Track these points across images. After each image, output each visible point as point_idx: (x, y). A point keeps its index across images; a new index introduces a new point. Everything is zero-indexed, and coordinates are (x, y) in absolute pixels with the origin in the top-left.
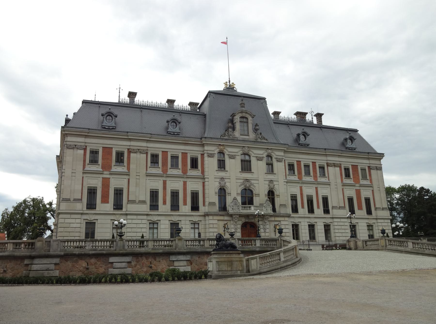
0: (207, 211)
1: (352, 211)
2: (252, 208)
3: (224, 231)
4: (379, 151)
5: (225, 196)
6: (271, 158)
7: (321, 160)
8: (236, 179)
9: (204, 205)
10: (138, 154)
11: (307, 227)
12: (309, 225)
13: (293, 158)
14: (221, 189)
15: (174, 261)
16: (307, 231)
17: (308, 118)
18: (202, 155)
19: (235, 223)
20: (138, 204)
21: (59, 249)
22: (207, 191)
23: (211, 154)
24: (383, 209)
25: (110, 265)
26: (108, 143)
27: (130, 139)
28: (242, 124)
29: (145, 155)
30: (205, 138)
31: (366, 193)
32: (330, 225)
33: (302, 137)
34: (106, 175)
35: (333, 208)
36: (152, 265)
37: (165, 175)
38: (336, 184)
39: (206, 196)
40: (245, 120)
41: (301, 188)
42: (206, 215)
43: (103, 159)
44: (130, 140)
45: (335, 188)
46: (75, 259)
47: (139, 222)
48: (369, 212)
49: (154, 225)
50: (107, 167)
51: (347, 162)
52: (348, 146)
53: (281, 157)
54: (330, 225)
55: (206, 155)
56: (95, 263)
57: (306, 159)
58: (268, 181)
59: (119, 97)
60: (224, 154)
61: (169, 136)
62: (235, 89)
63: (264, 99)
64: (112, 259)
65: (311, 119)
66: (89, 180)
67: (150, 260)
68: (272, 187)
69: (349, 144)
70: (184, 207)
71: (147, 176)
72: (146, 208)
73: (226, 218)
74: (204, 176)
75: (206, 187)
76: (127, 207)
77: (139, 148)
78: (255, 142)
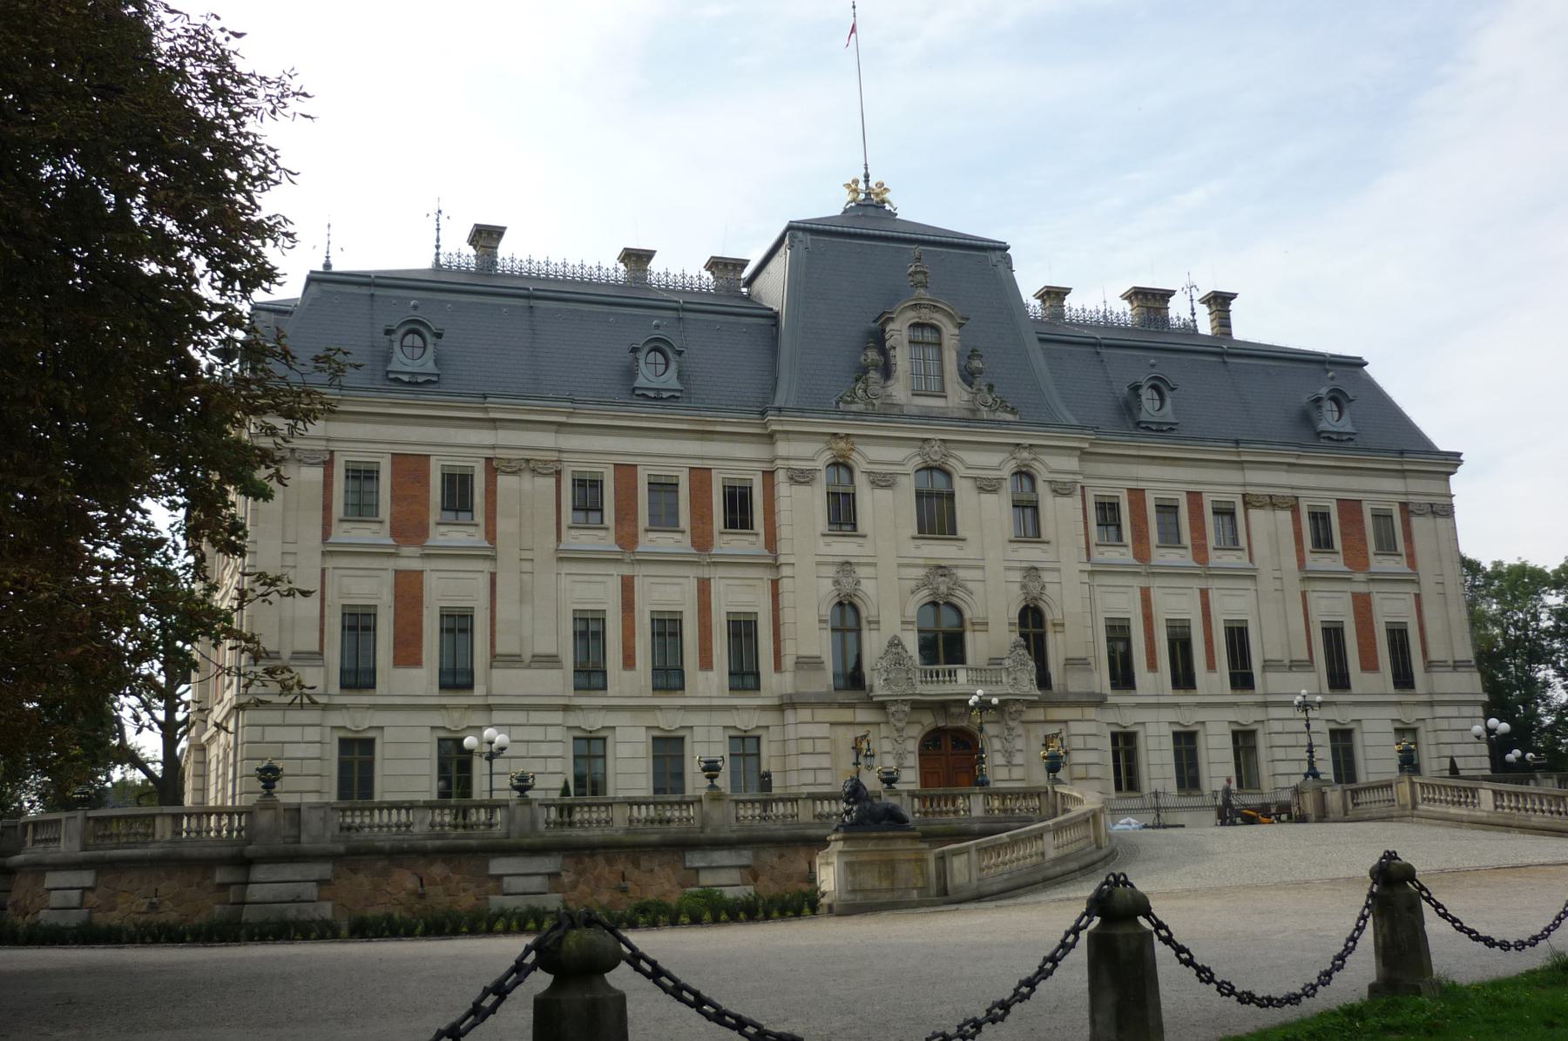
0: (790, 690)
1: (1339, 679)
2: (962, 676)
3: (857, 764)
4: (1443, 446)
5: (858, 631)
6: (1032, 478)
7: (1221, 484)
8: (900, 565)
9: (778, 667)
10: (527, 476)
11: (1169, 743)
12: (1177, 736)
13: (1113, 479)
14: (840, 604)
15: (697, 870)
16: (1169, 757)
17: (1178, 310)
18: (769, 475)
19: (896, 734)
20: (529, 667)
21: (328, 835)
22: (787, 616)
23: (802, 471)
24: (1457, 666)
25: (491, 884)
26: (412, 437)
27: (494, 420)
28: (919, 350)
29: (552, 481)
30: (780, 409)
31: (1391, 607)
32: (1253, 733)
33: (1147, 394)
34: (410, 561)
35: (1267, 665)
36: (629, 884)
37: (627, 557)
38: (1278, 574)
39: (786, 632)
40: (928, 336)
41: (1146, 595)
42: (786, 705)
43: (394, 498)
44: (494, 423)
45: (1272, 592)
46: (380, 864)
47: (537, 734)
48: (1403, 679)
50: (409, 529)
51: (1322, 487)
52: (1323, 426)
53: (1069, 478)
54: (1253, 733)
55: (781, 476)
56: (446, 879)
57: (1164, 480)
58: (1021, 569)
59: (438, 247)
60: (850, 470)
61: (643, 406)
62: (888, 207)
63: (1003, 248)
64: (498, 866)
65: (1187, 316)
66: (346, 581)
67: (620, 867)
68: (1035, 593)
69: (1329, 420)
70: (701, 675)
71: (560, 559)
72: (557, 682)
73: (863, 715)
74: (776, 559)
75: (786, 600)
76: (491, 682)
78: (968, 420)
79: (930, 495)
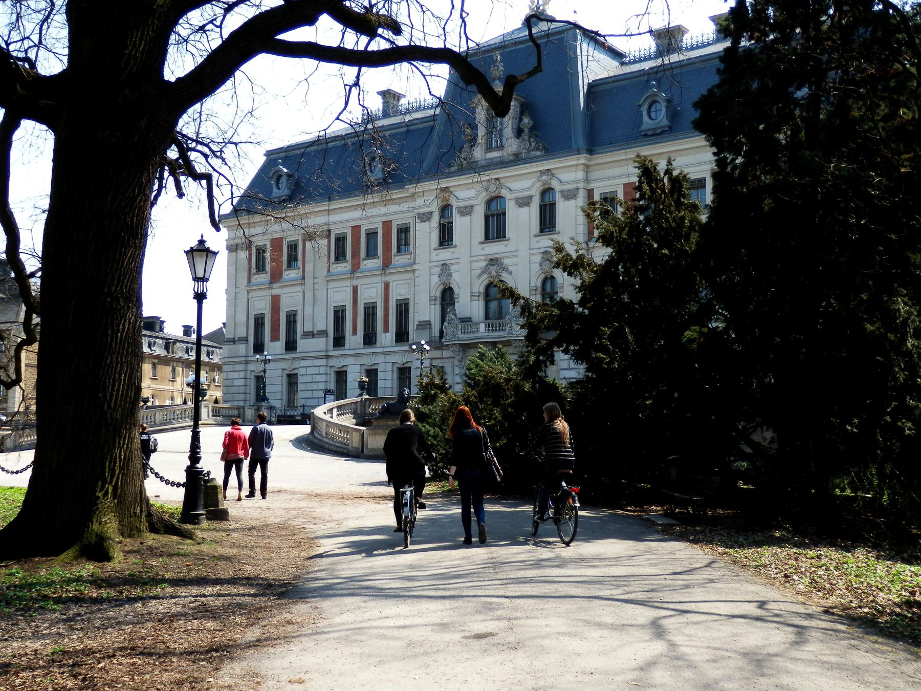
23: (424, 214)
49: (341, 376)
70: (383, 335)
73: (446, 353)
76: (303, 345)
79: (493, 216)
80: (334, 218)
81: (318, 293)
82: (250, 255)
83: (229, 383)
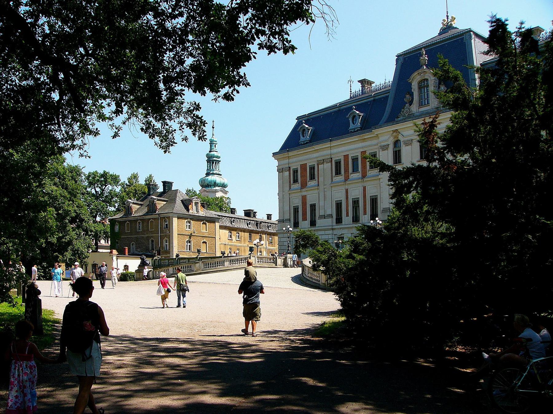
29: (330, 164)
76: (320, 222)
77: (324, 158)
80: (334, 151)
81: (326, 194)
82: (290, 174)
83: (281, 243)
